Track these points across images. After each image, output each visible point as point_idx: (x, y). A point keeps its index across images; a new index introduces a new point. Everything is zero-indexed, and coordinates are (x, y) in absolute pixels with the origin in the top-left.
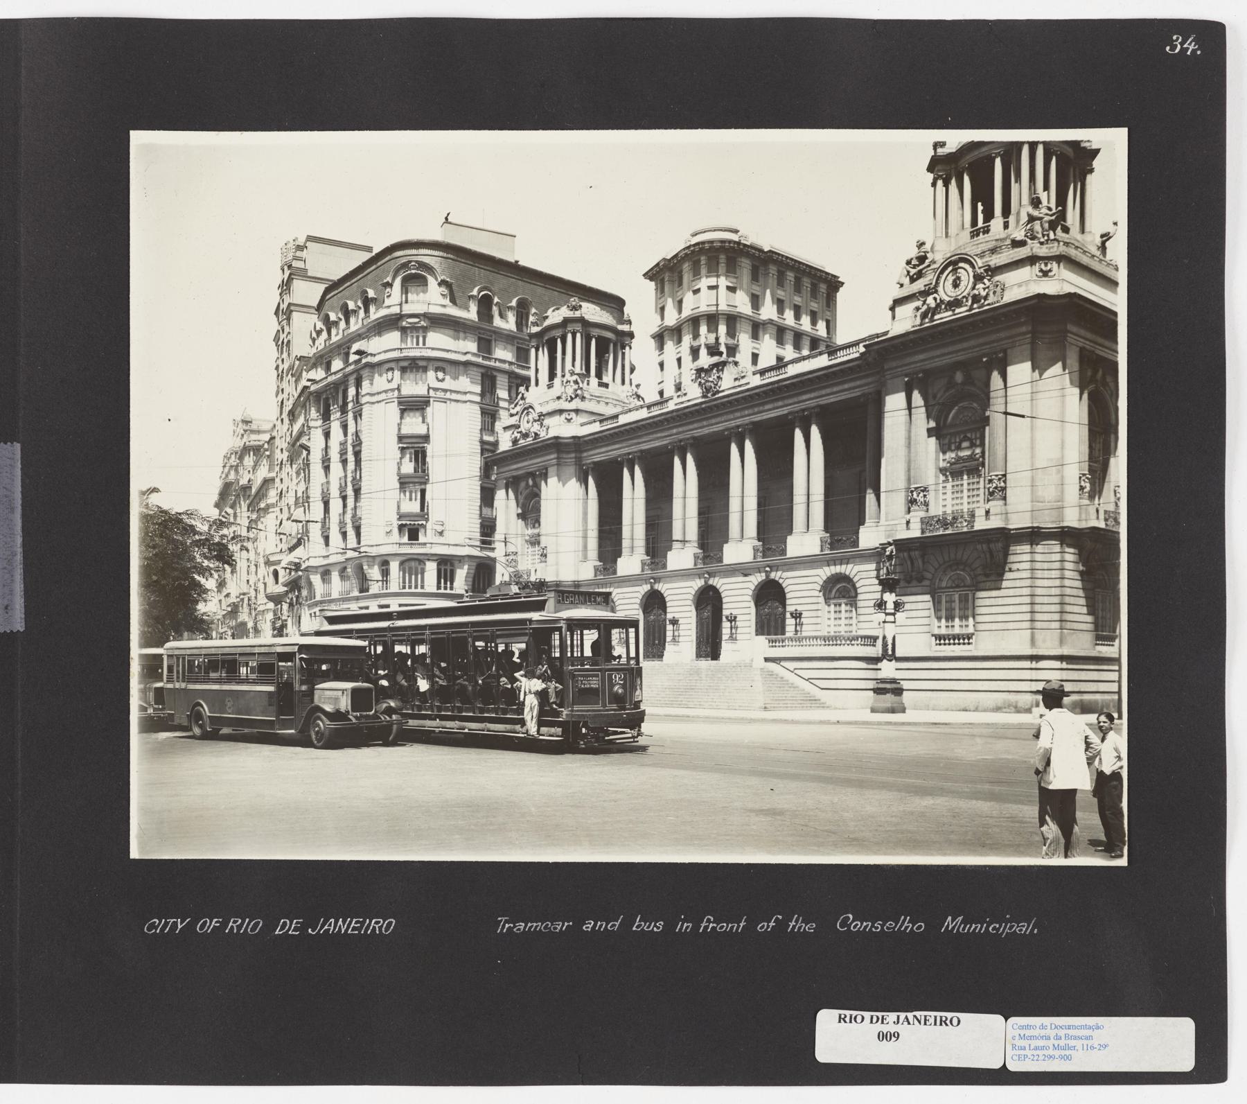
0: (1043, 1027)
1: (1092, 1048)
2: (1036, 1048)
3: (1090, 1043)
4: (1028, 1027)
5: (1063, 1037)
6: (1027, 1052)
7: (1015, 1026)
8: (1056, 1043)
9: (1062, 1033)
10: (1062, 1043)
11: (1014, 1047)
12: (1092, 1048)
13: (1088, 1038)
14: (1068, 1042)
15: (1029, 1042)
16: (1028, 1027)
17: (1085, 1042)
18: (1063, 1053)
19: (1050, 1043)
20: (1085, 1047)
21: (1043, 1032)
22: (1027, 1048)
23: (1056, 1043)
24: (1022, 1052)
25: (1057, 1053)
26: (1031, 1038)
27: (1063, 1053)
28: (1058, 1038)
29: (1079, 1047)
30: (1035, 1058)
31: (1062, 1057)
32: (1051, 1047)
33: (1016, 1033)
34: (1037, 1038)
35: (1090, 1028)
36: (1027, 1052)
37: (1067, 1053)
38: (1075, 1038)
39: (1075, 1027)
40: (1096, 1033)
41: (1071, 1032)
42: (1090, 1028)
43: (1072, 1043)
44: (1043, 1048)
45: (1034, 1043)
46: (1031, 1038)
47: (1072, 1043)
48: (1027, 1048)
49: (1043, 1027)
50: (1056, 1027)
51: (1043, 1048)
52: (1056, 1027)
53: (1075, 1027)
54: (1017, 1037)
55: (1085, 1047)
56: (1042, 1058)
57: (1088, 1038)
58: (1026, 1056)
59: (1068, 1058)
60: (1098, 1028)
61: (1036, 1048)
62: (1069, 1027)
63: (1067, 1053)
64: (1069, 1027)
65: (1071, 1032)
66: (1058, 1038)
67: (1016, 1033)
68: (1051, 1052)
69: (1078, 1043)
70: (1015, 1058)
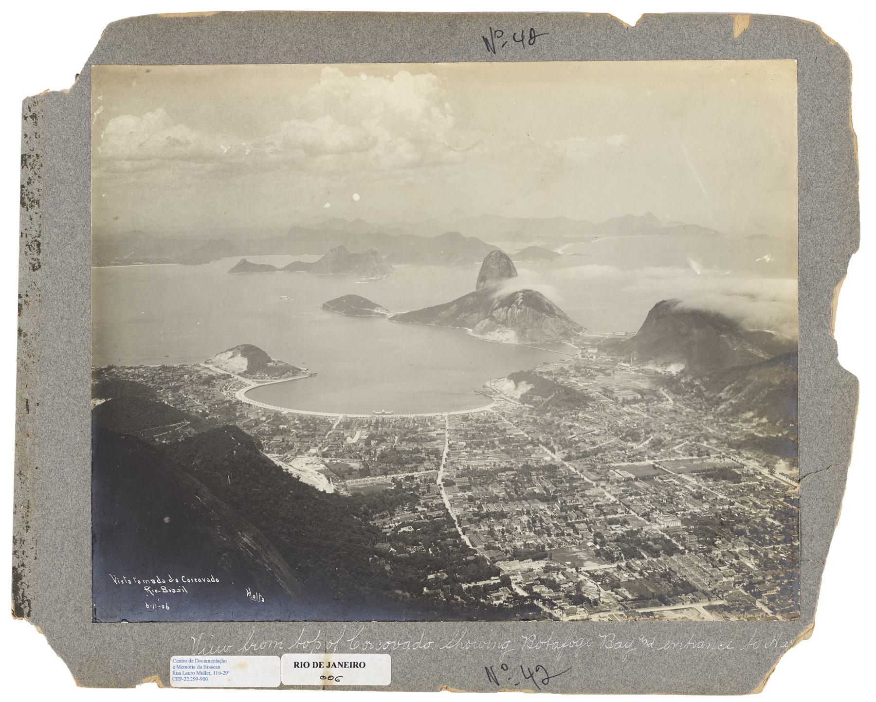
0: (191, 661)
1: (220, 673)
2: (187, 674)
3: (218, 670)
4: (182, 661)
5: (203, 667)
6: (183, 676)
7: (175, 661)
8: (199, 670)
9: (202, 664)
10: (202, 670)
13: (217, 668)
14: (205, 670)
15: (184, 670)
16: (182, 661)
17: (216, 670)
18: (203, 676)
20: (216, 673)
21: (191, 664)
22: (182, 674)
23: (199, 670)
25: (199, 676)
27: (203, 676)
28: (200, 667)
29: (212, 673)
31: (202, 679)
32: (196, 672)
33: (175, 664)
34: (187, 668)
35: (219, 661)
36: (183, 676)
37: (205, 676)
38: (210, 668)
40: (222, 665)
41: (208, 664)
42: (219, 661)
43: (208, 670)
44: (191, 673)
45: (186, 670)
47: (208, 670)
48: (182, 674)
49: (191, 661)
50: (199, 661)
51: (191, 673)
52: (199, 661)
53: (210, 661)
54: (176, 667)
55: (216, 673)
56: (190, 679)
57: (217, 668)
58: (181, 678)
59: (206, 679)
60: (224, 662)
61: (187, 674)
62: (206, 661)
63: (205, 676)
64: (206, 661)
65: (208, 664)
66: (200, 667)
67: (175, 664)
68: (196, 676)
70: (174, 679)
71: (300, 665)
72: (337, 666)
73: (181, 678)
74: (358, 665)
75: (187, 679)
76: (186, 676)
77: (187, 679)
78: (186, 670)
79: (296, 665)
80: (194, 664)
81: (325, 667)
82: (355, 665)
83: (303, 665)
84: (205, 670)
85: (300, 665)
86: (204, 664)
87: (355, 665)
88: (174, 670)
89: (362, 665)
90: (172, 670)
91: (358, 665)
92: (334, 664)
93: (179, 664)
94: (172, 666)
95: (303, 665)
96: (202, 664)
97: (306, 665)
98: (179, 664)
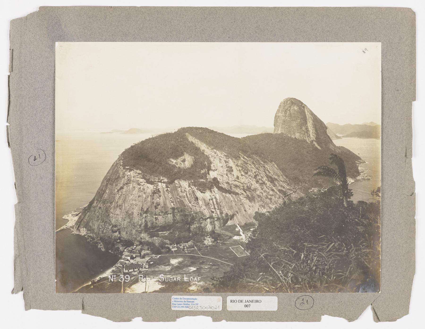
1: (194, 304)
2: (179, 304)
3: (193, 303)
4: (177, 299)
7: (173, 298)
9: (186, 300)
10: (186, 303)
11: (173, 304)
12: (194, 304)
13: (193, 302)
14: (187, 303)
17: (192, 303)
18: (186, 306)
19: (182, 303)
21: (181, 300)
22: (176, 304)
24: (175, 305)
25: (184, 306)
26: (177, 301)
27: (186, 306)
30: (178, 307)
31: (186, 307)
32: (183, 304)
33: (174, 300)
34: (179, 302)
35: (194, 299)
36: (177, 305)
37: (187, 306)
38: (189, 302)
39: (190, 299)
41: (189, 300)
42: (194, 299)
43: (189, 303)
44: (181, 304)
45: (178, 303)
46: (177, 301)
48: (176, 304)
49: (181, 299)
51: (181, 304)
53: (190, 299)
54: (174, 301)
57: (193, 302)
58: (176, 307)
59: (187, 307)
60: (196, 299)
61: (179, 304)
63: (187, 306)
64: (188, 299)
65: (189, 300)
67: (174, 300)
68: (183, 305)
69: (190, 303)
71: (233, 301)
72: (249, 302)
73: (176, 307)
74: (258, 302)
75: (179, 307)
76: (179, 306)
77: (179, 307)
78: (178, 303)
79: (231, 301)
80: (182, 300)
81: (244, 303)
82: (257, 301)
83: (234, 301)
84: (187, 303)
85: (233, 301)
86: (187, 300)
87: (257, 301)
88: (173, 303)
89: (260, 301)
90: (172, 303)
91: (258, 302)
92: (248, 301)
93: (175, 300)
94: (172, 300)
95: (234, 301)
96: (186, 300)
97: (236, 301)
98: (175, 300)
